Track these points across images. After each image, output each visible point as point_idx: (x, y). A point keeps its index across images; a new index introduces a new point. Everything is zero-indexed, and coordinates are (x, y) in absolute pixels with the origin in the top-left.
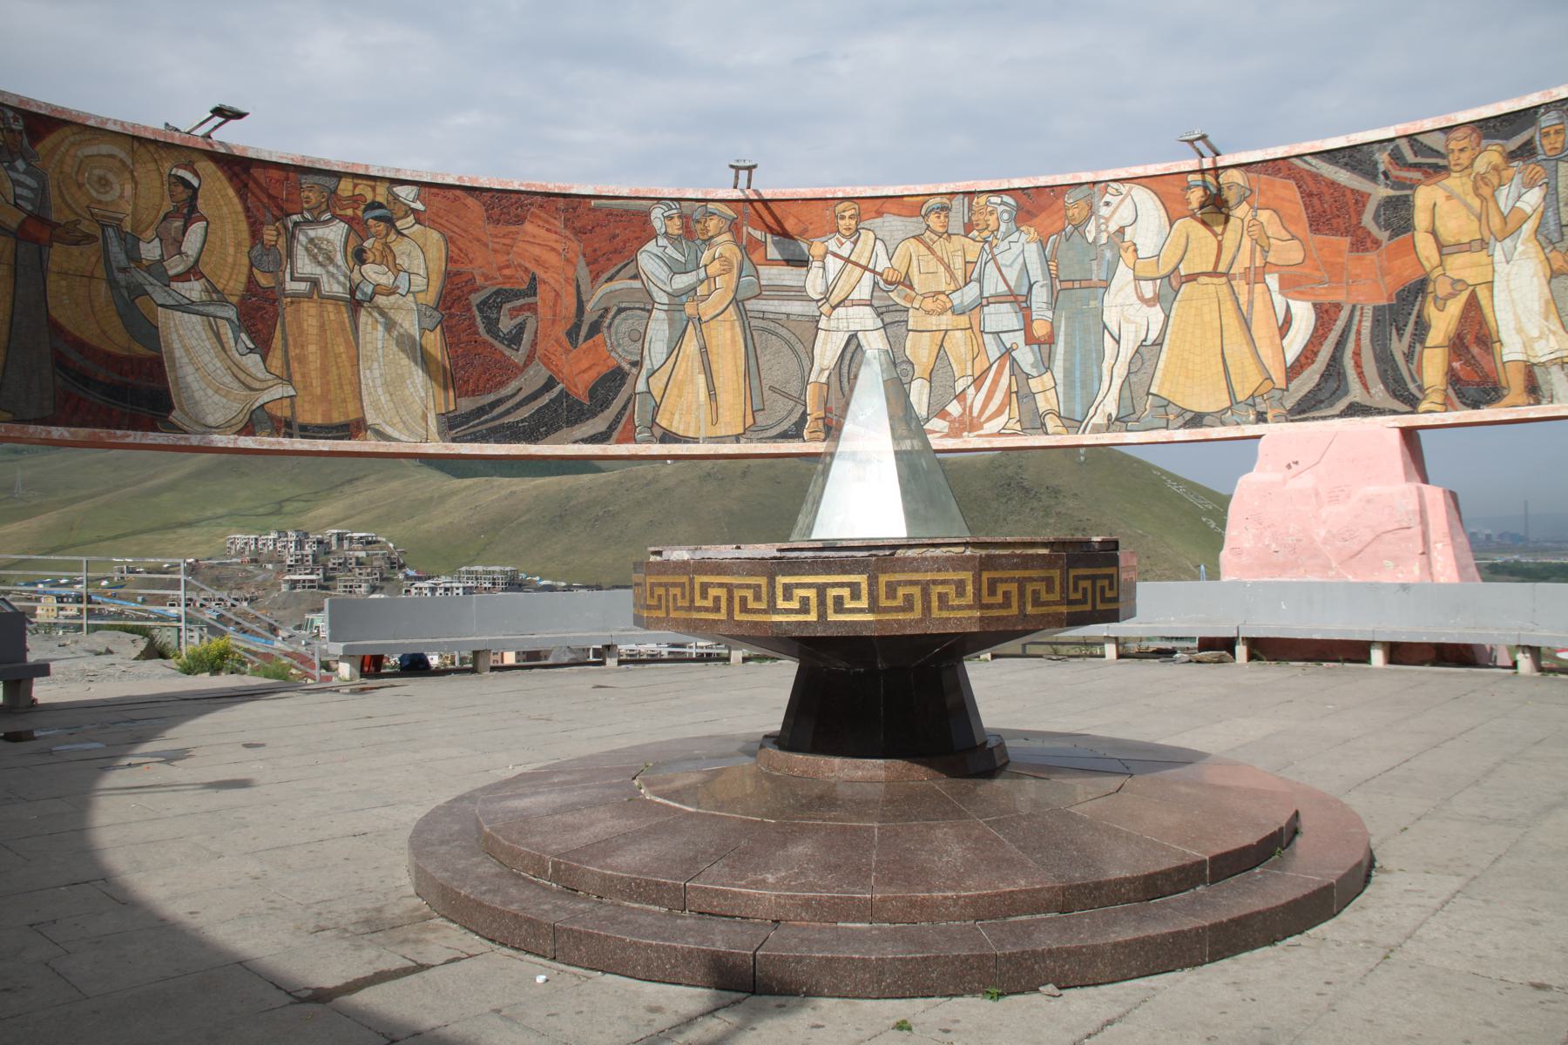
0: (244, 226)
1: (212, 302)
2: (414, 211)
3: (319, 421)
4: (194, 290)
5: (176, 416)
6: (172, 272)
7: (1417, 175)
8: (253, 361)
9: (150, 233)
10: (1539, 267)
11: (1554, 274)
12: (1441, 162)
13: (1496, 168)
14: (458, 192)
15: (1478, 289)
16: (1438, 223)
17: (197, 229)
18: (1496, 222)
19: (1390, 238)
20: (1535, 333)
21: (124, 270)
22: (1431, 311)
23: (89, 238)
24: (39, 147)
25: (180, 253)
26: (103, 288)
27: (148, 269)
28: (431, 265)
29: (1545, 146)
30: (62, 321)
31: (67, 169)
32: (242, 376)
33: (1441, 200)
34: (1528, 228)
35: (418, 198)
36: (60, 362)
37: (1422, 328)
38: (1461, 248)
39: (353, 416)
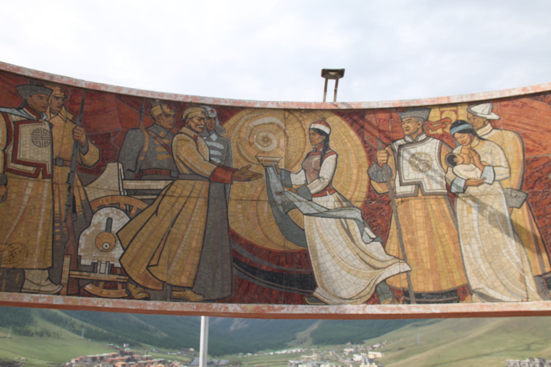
0: (363, 154)
1: (342, 208)
2: (490, 121)
3: (431, 289)
4: (329, 201)
5: (318, 292)
6: (313, 191)
8: (376, 248)
9: (298, 168)
14: (524, 100)
17: (329, 161)
21: (280, 193)
23: (256, 176)
24: (226, 125)
25: (319, 178)
26: (266, 207)
27: (297, 191)
28: (510, 158)
30: (238, 231)
31: (242, 135)
32: (367, 259)
35: (492, 110)
36: (236, 259)
39: (459, 283)
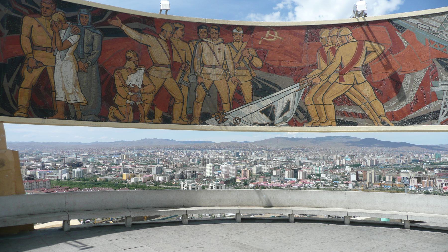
7: (26, 11)
10: (74, 66)
11: (79, 71)
12: (37, 9)
13: (61, 21)
15: (48, 68)
16: (32, 34)
18: (58, 43)
19: (8, 34)
20: (70, 91)
22: (25, 72)
29: (82, 21)
33: (35, 26)
34: (71, 49)
37: (20, 79)
38: (41, 48)
